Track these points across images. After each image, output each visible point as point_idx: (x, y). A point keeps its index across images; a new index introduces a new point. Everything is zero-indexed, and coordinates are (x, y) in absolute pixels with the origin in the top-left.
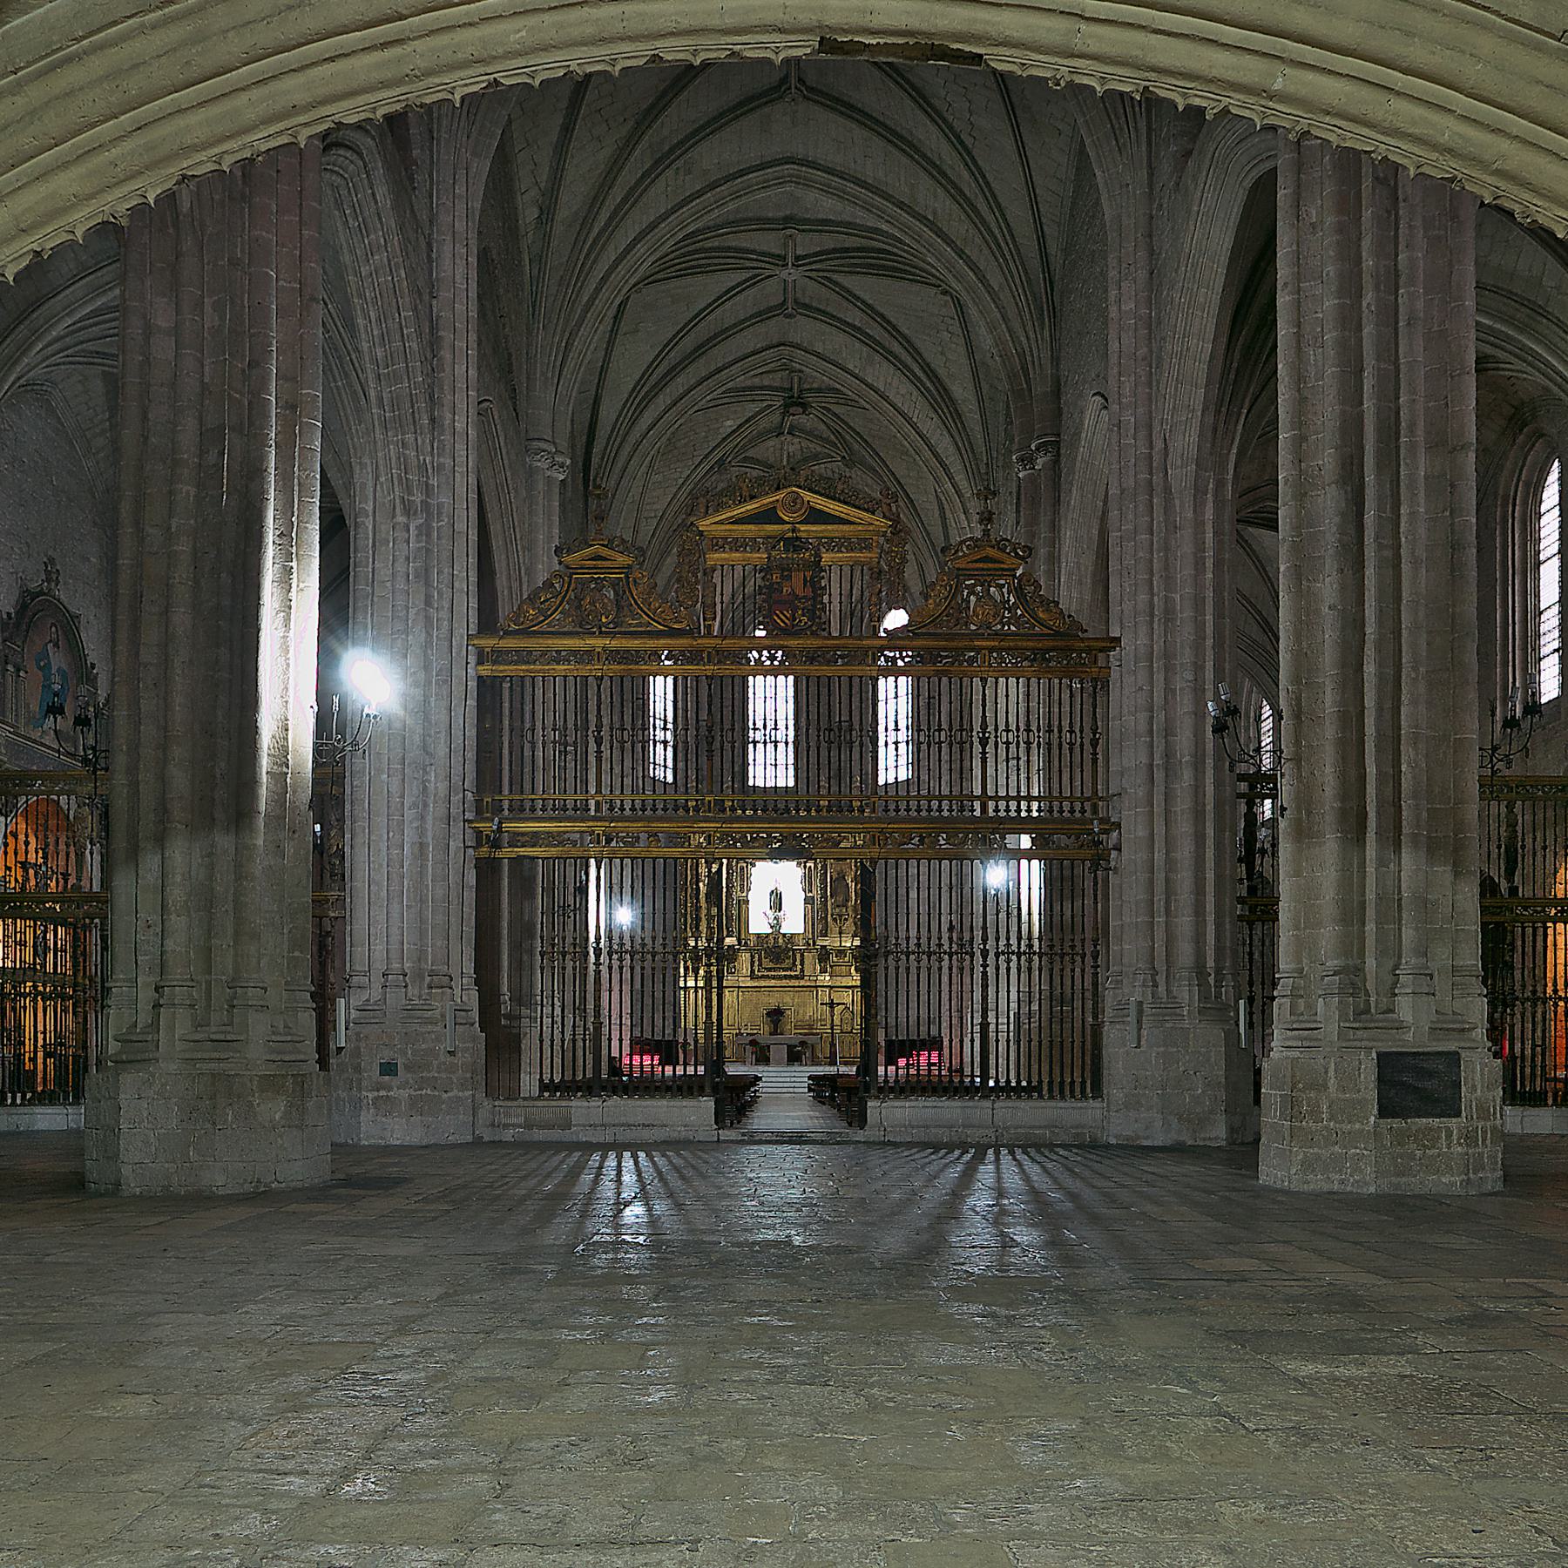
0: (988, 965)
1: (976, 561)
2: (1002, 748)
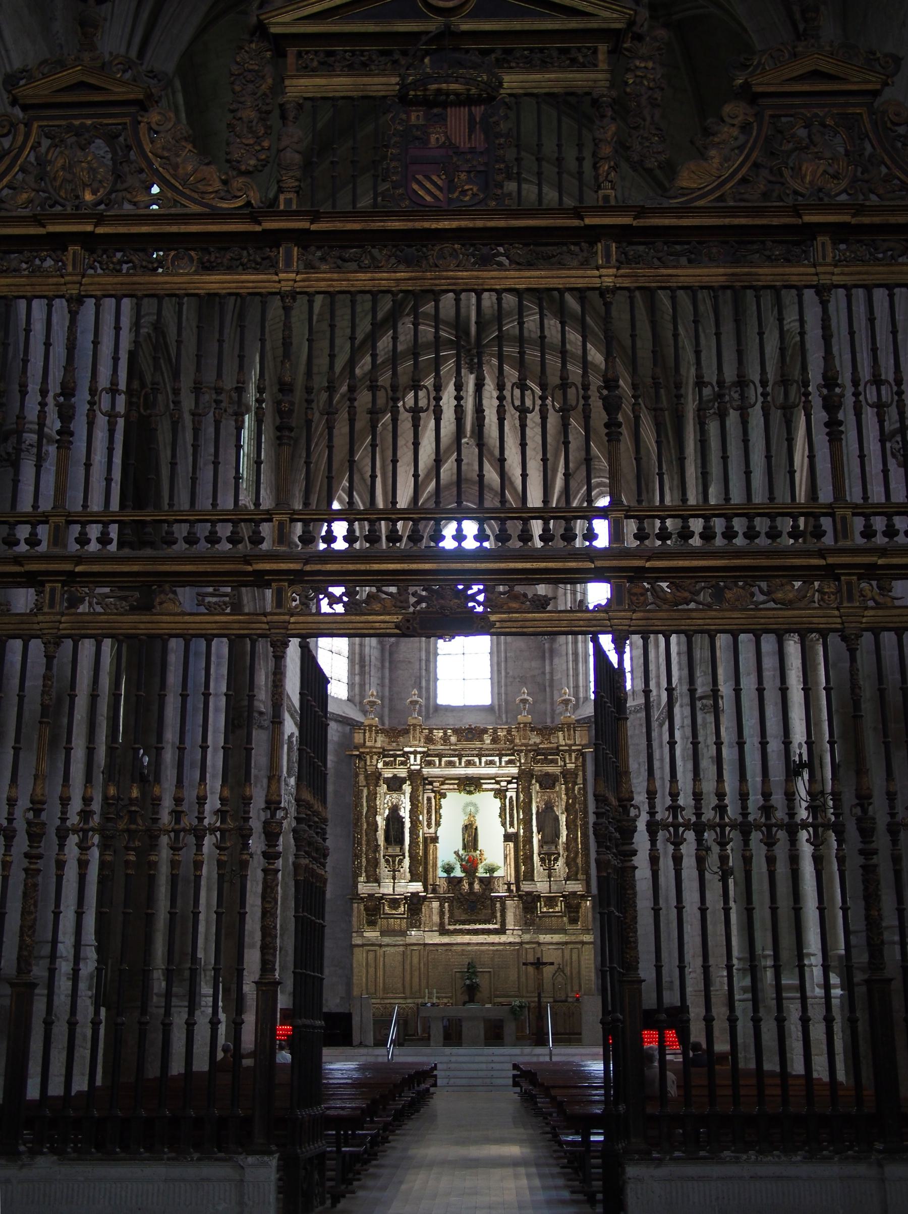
0: (875, 852)
1: (801, 78)
2: (869, 415)
